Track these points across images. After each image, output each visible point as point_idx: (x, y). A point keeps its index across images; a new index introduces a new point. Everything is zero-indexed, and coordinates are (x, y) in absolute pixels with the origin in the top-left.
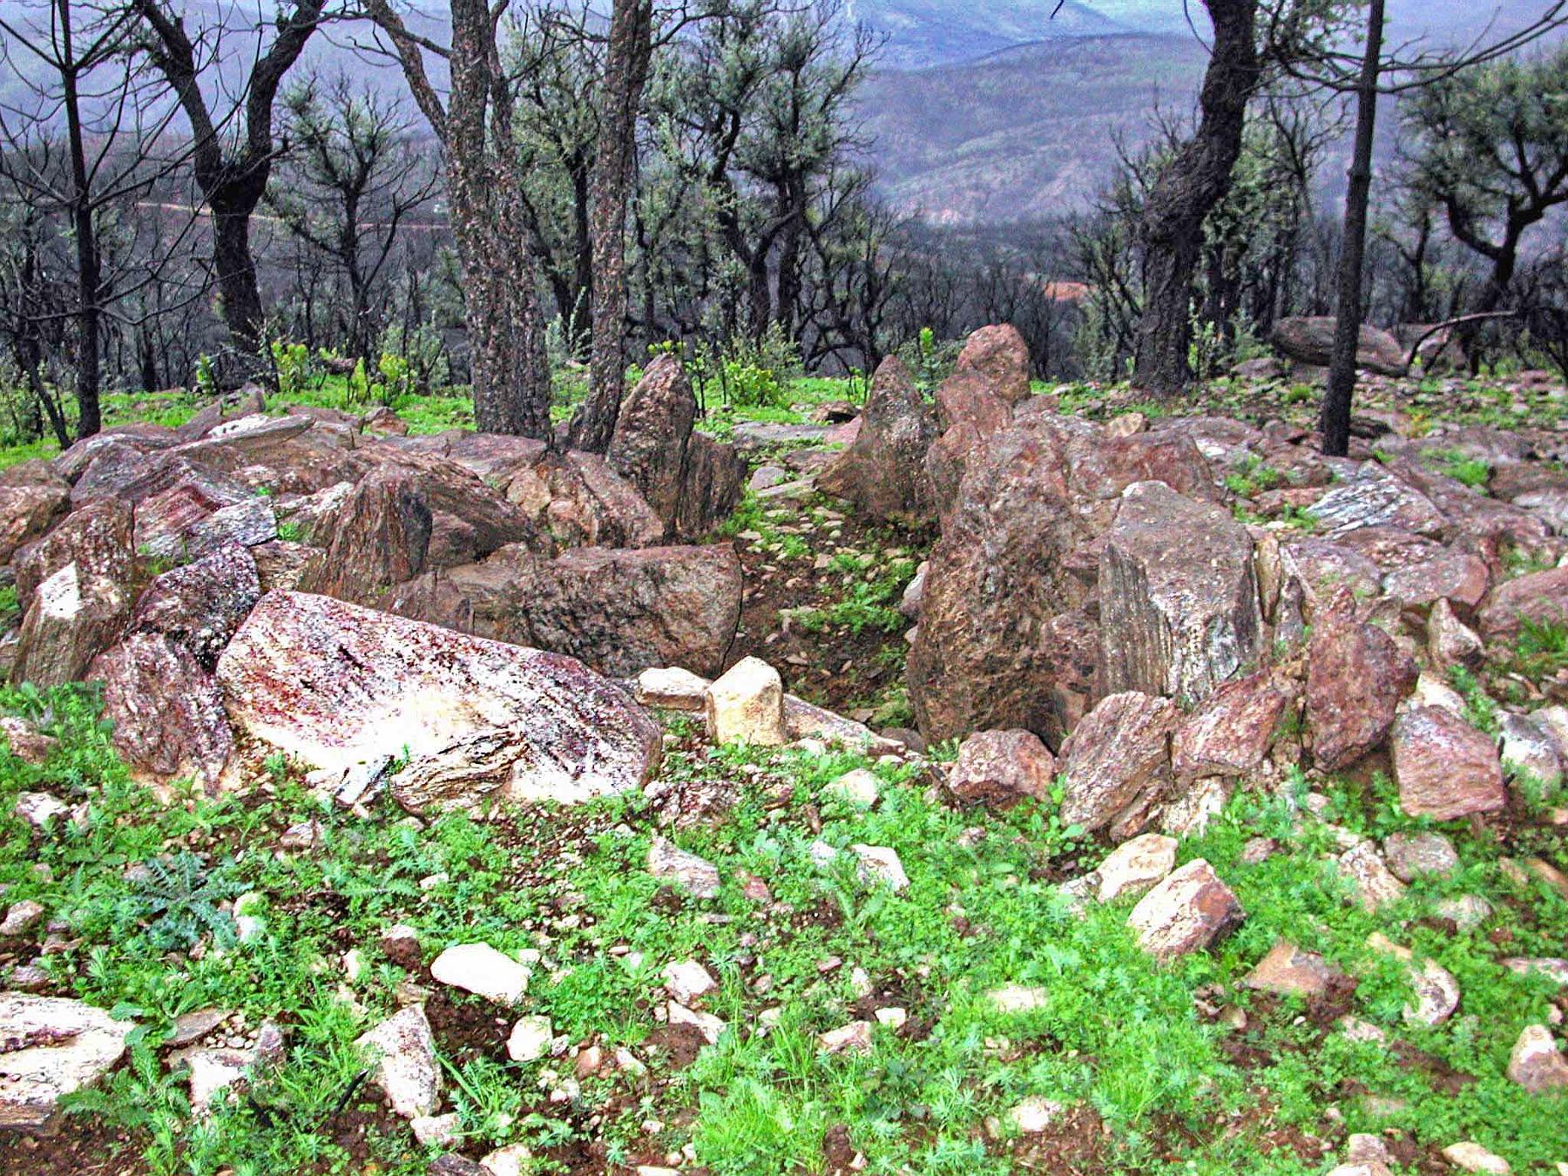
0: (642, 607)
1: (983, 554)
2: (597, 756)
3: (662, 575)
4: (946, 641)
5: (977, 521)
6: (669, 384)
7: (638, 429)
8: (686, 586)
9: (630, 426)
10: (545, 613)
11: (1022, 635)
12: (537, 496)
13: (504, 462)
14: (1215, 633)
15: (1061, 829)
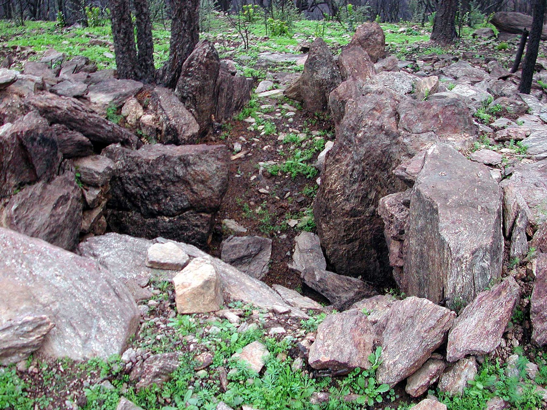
0: (178, 177)
1: (352, 158)
2: (99, 328)
3: (189, 163)
4: (332, 198)
5: (350, 141)
6: (205, 55)
7: (189, 76)
8: (201, 168)
9: (186, 75)
10: (130, 179)
11: (371, 200)
12: (135, 112)
13: (120, 95)
14: (478, 259)
15: (377, 386)
